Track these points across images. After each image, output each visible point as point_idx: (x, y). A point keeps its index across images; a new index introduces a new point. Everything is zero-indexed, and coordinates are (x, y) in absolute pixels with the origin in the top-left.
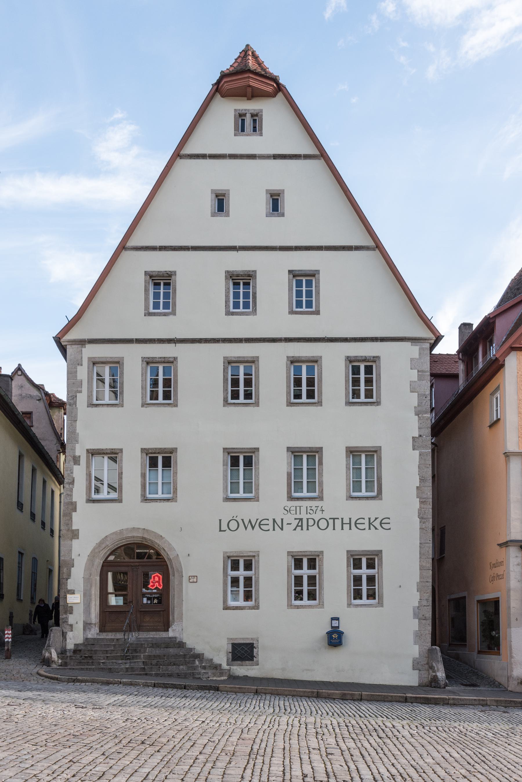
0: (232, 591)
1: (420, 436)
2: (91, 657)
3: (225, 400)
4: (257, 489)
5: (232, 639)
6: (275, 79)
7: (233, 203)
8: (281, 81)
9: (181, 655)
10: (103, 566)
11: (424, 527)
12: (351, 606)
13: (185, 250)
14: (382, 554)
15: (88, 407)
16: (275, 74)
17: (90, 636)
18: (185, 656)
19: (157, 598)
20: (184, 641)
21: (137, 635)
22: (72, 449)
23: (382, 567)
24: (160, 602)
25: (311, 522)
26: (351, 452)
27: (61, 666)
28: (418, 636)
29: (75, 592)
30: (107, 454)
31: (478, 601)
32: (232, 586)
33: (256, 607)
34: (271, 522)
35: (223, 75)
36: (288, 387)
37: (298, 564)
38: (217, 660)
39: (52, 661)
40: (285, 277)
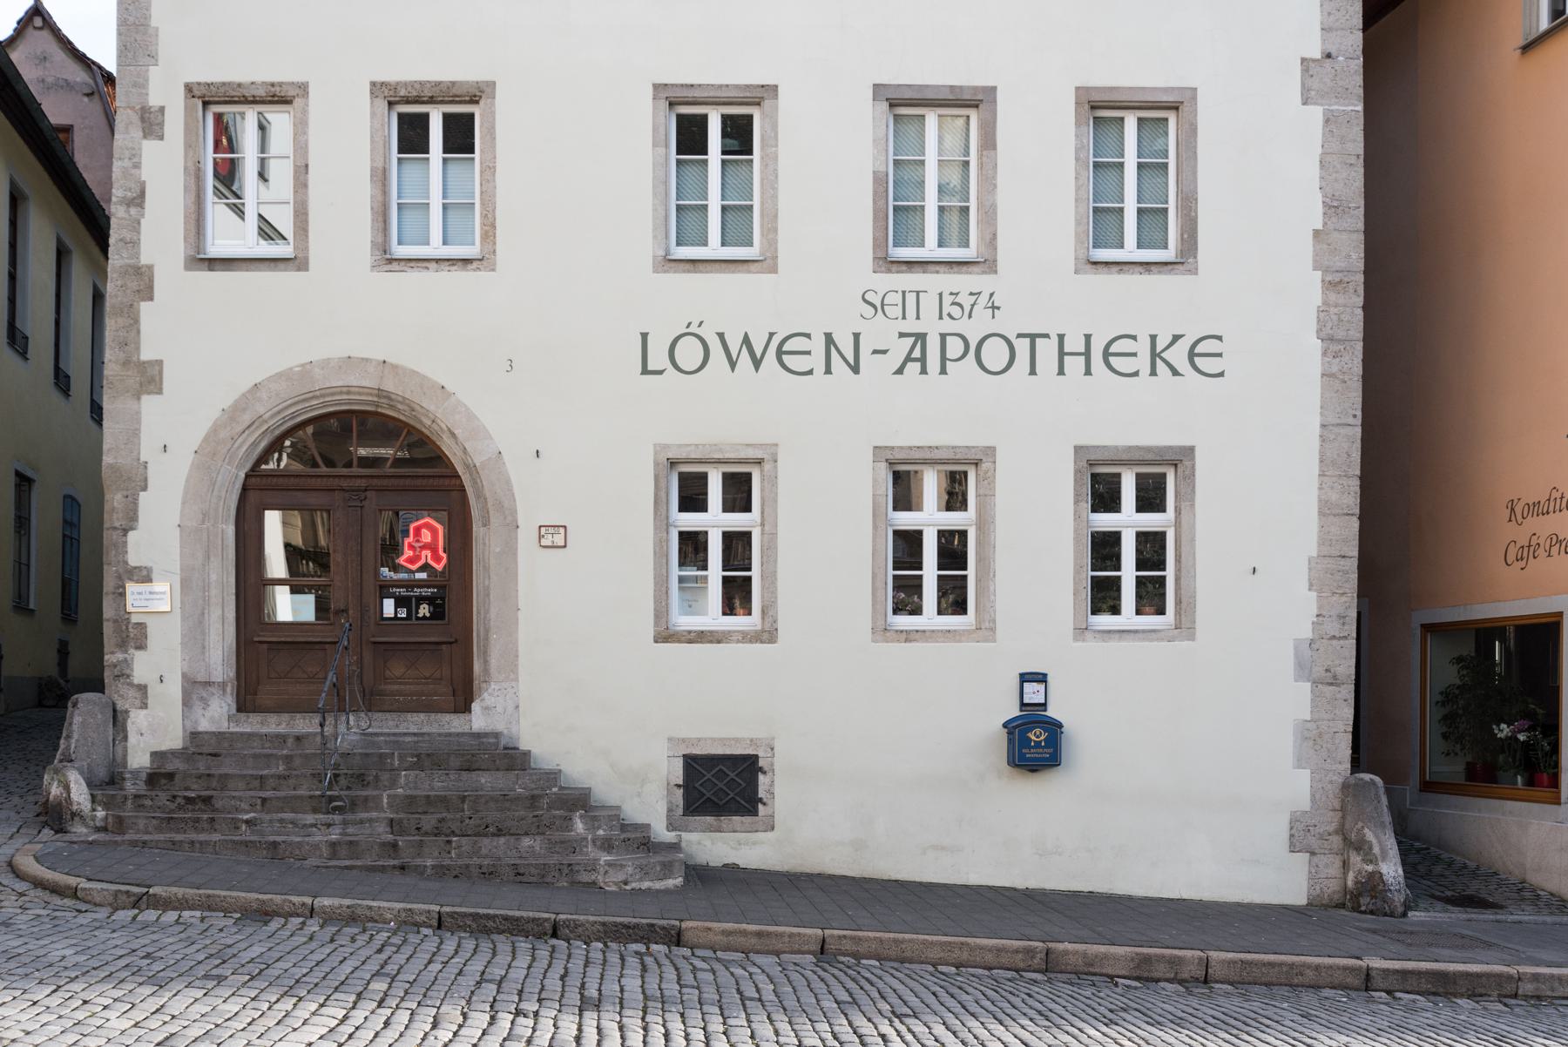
0: (681, 580)
1: (1329, 56)
2: (207, 800)
4: (771, 230)
5: (683, 740)
10: (245, 489)
11: (1335, 369)
12: (1088, 635)
14: (1193, 459)
17: (204, 725)
19: (430, 600)
20: (523, 746)
21: (364, 725)
22: (135, 85)
23: (1193, 506)
24: (438, 614)
25: (954, 347)
28: (1310, 737)
29: (154, 576)
30: (254, 101)
32: (682, 564)
33: (767, 635)
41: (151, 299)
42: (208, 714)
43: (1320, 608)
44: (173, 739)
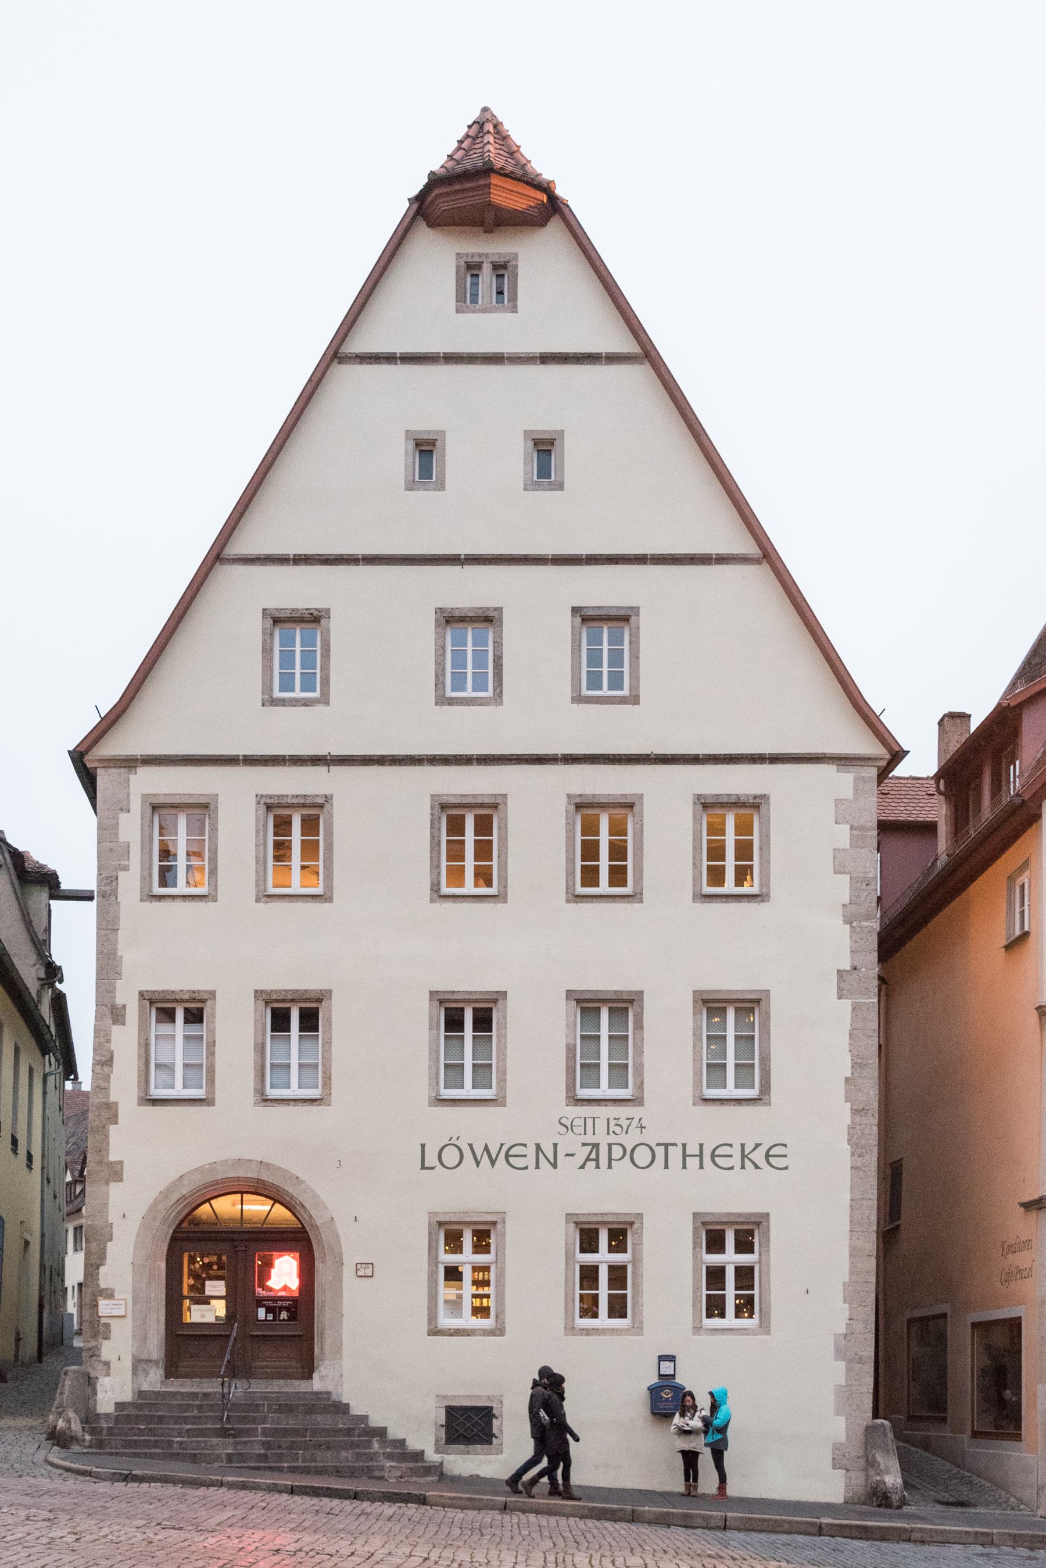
3: (435, 888)
4: (502, 1081)
6: (546, 188)
7: (454, 458)
8: (559, 192)
9: (341, 1430)
12: (702, 1332)
13: (349, 564)
14: (768, 1221)
15: (142, 900)
16: (547, 175)
17: (146, 1387)
18: (349, 1432)
19: (288, 1309)
21: (246, 1387)
23: (768, 1250)
24: (292, 1317)
25: (617, 1152)
26: (705, 1001)
27: (90, 1447)
28: (845, 1395)
31: (975, 1325)
33: (499, 1331)
34: (531, 1151)
35: (435, 181)
36: (570, 861)
37: (588, 1241)
38: (414, 1444)
39: (72, 1438)
40: (566, 622)
41: (116, 1123)
42: (148, 1379)
43: (851, 1314)
44: (127, 1396)
